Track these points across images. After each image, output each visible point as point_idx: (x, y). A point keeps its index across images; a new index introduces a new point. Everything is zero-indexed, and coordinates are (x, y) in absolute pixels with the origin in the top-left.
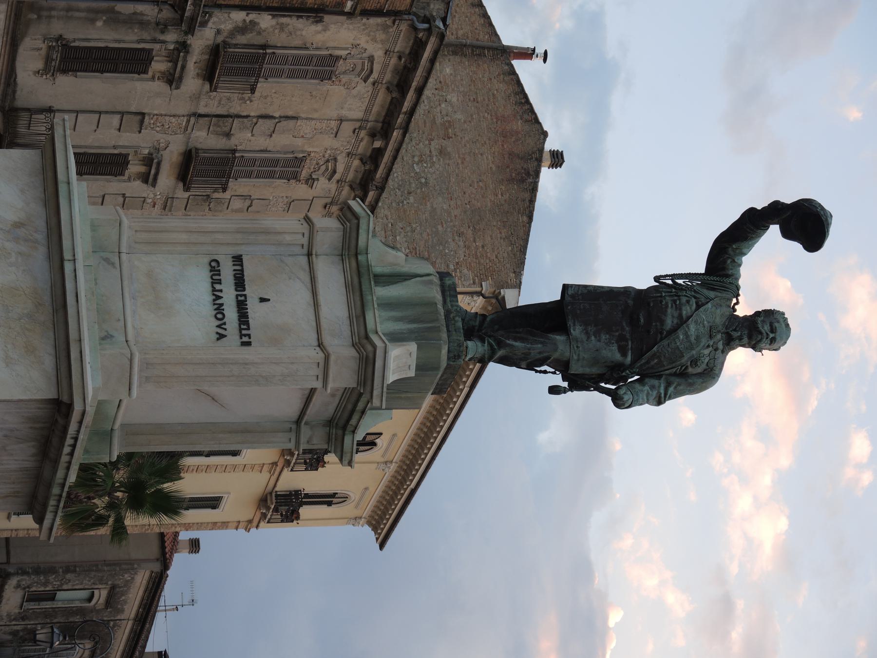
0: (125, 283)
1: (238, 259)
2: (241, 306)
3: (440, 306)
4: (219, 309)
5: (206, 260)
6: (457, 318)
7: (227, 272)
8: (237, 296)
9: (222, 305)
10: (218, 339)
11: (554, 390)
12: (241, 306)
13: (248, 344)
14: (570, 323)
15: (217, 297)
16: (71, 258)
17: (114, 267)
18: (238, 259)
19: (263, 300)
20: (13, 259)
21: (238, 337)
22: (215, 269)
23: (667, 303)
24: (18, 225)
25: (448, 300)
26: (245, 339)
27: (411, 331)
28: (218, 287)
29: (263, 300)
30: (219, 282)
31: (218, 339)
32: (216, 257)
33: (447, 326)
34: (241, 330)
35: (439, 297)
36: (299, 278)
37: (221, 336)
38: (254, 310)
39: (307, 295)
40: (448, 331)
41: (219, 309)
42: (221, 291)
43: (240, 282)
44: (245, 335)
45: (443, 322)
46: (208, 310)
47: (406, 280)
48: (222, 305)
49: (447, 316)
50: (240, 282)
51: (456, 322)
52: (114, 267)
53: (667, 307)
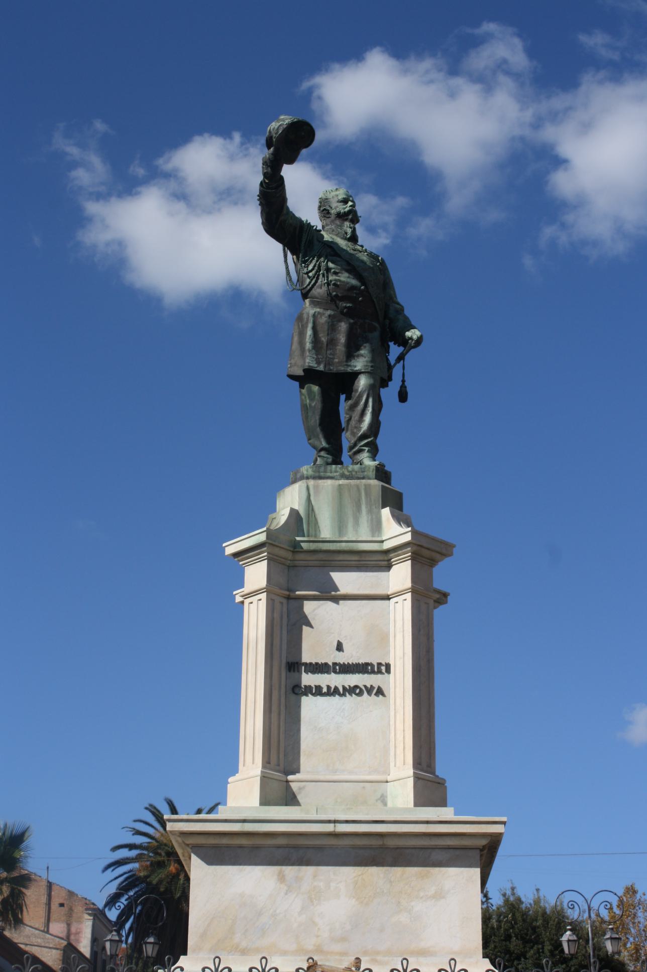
0: (321, 778)
3: (341, 482)
6: (350, 469)
8: (335, 672)
9: (344, 687)
10: (383, 695)
11: (403, 396)
13: (388, 666)
14: (349, 370)
15: (333, 692)
16: (332, 825)
17: (304, 787)
20: (321, 884)
21: (379, 675)
23: (335, 280)
25: (329, 474)
26: (383, 668)
27: (370, 511)
28: (325, 690)
29: (340, 647)
31: (383, 695)
33: (358, 478)
34: (373, 672)
35: (329, 482)
36: (314, 610)
37: (380, 692)
40: (363, 478)
42: (329, 687)
44: (379, 668)
45: (353, 482)
46: (349, 700)
47: (313, 510)
48: (344, 687)
49: (348, 478)
51: (353, 470)
52: (304, 787)
53: (340, 281)
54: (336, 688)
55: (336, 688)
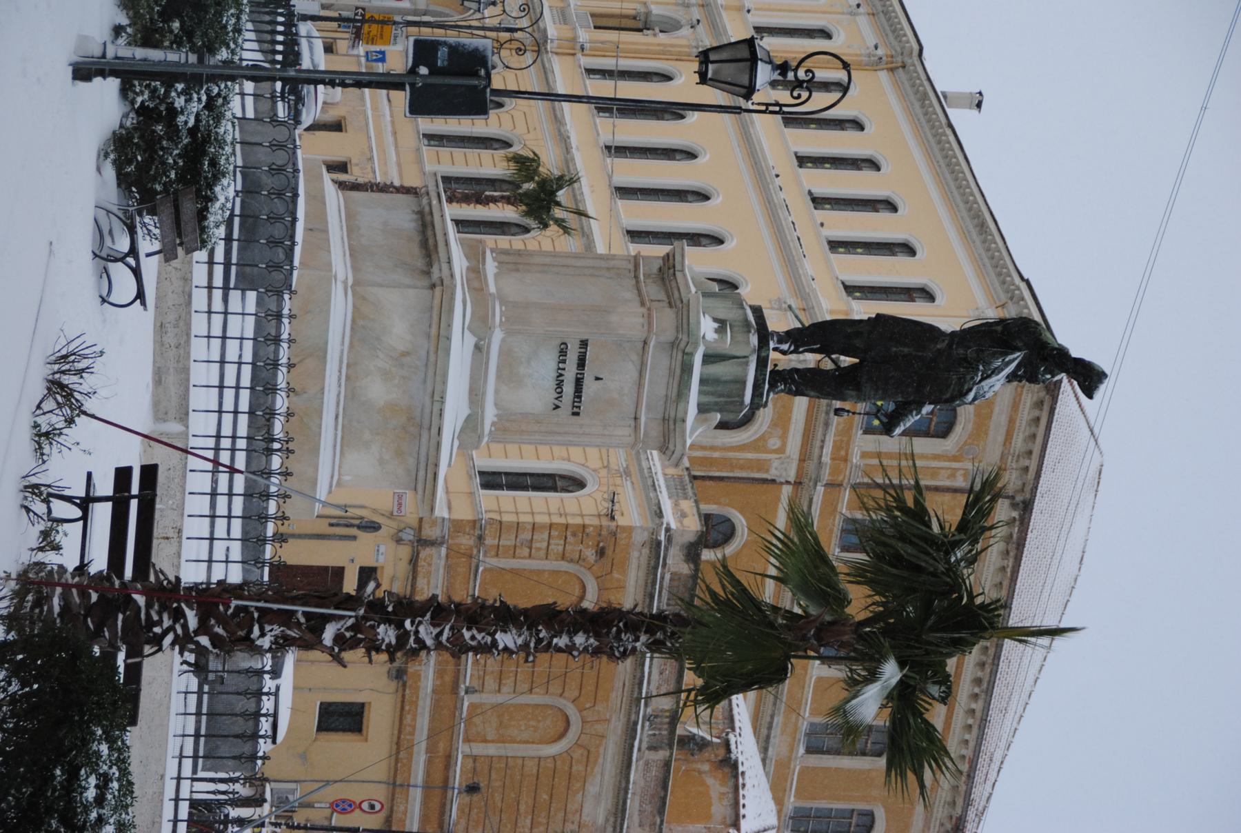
1: (584, 344)
2: (579, 383)
4: (560, 385)
5: (559, 342)
7: (572, 358)
12: (579, 383)
13: (577, 414)
18: (584, 344)
19: (597, 379)
20: (396, 382)
22: (563, 352)
24: (405, 354)
26: (575, 410)
27: (716, 403)
29: (597, 379)
30: (564, 362)
32: (565, 340)
37: (557, 407)
38: (590, 387)
39: (635, 375)
41: (560, 385)
43: (581, 363)
46: (553, 384)
50: (581, 363)
54: (561, 375)
55: (561, 375)
